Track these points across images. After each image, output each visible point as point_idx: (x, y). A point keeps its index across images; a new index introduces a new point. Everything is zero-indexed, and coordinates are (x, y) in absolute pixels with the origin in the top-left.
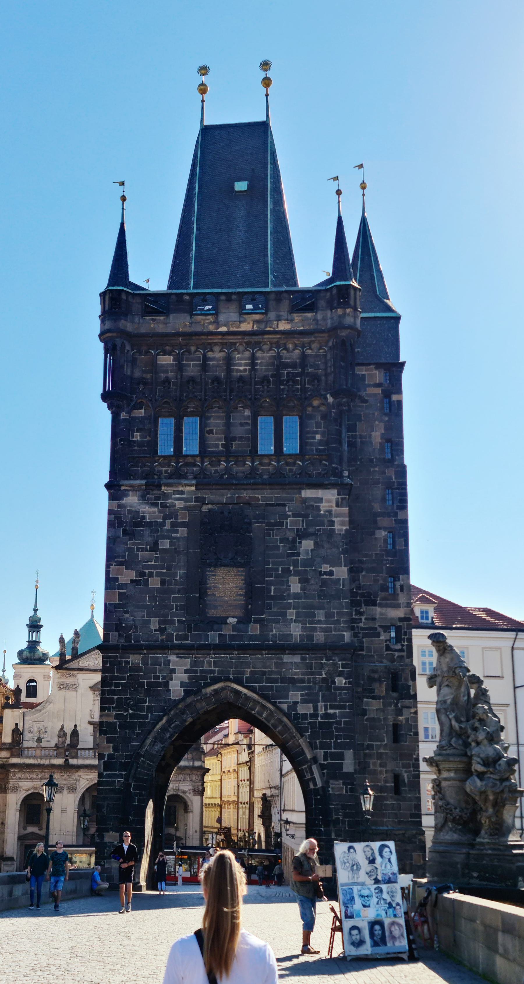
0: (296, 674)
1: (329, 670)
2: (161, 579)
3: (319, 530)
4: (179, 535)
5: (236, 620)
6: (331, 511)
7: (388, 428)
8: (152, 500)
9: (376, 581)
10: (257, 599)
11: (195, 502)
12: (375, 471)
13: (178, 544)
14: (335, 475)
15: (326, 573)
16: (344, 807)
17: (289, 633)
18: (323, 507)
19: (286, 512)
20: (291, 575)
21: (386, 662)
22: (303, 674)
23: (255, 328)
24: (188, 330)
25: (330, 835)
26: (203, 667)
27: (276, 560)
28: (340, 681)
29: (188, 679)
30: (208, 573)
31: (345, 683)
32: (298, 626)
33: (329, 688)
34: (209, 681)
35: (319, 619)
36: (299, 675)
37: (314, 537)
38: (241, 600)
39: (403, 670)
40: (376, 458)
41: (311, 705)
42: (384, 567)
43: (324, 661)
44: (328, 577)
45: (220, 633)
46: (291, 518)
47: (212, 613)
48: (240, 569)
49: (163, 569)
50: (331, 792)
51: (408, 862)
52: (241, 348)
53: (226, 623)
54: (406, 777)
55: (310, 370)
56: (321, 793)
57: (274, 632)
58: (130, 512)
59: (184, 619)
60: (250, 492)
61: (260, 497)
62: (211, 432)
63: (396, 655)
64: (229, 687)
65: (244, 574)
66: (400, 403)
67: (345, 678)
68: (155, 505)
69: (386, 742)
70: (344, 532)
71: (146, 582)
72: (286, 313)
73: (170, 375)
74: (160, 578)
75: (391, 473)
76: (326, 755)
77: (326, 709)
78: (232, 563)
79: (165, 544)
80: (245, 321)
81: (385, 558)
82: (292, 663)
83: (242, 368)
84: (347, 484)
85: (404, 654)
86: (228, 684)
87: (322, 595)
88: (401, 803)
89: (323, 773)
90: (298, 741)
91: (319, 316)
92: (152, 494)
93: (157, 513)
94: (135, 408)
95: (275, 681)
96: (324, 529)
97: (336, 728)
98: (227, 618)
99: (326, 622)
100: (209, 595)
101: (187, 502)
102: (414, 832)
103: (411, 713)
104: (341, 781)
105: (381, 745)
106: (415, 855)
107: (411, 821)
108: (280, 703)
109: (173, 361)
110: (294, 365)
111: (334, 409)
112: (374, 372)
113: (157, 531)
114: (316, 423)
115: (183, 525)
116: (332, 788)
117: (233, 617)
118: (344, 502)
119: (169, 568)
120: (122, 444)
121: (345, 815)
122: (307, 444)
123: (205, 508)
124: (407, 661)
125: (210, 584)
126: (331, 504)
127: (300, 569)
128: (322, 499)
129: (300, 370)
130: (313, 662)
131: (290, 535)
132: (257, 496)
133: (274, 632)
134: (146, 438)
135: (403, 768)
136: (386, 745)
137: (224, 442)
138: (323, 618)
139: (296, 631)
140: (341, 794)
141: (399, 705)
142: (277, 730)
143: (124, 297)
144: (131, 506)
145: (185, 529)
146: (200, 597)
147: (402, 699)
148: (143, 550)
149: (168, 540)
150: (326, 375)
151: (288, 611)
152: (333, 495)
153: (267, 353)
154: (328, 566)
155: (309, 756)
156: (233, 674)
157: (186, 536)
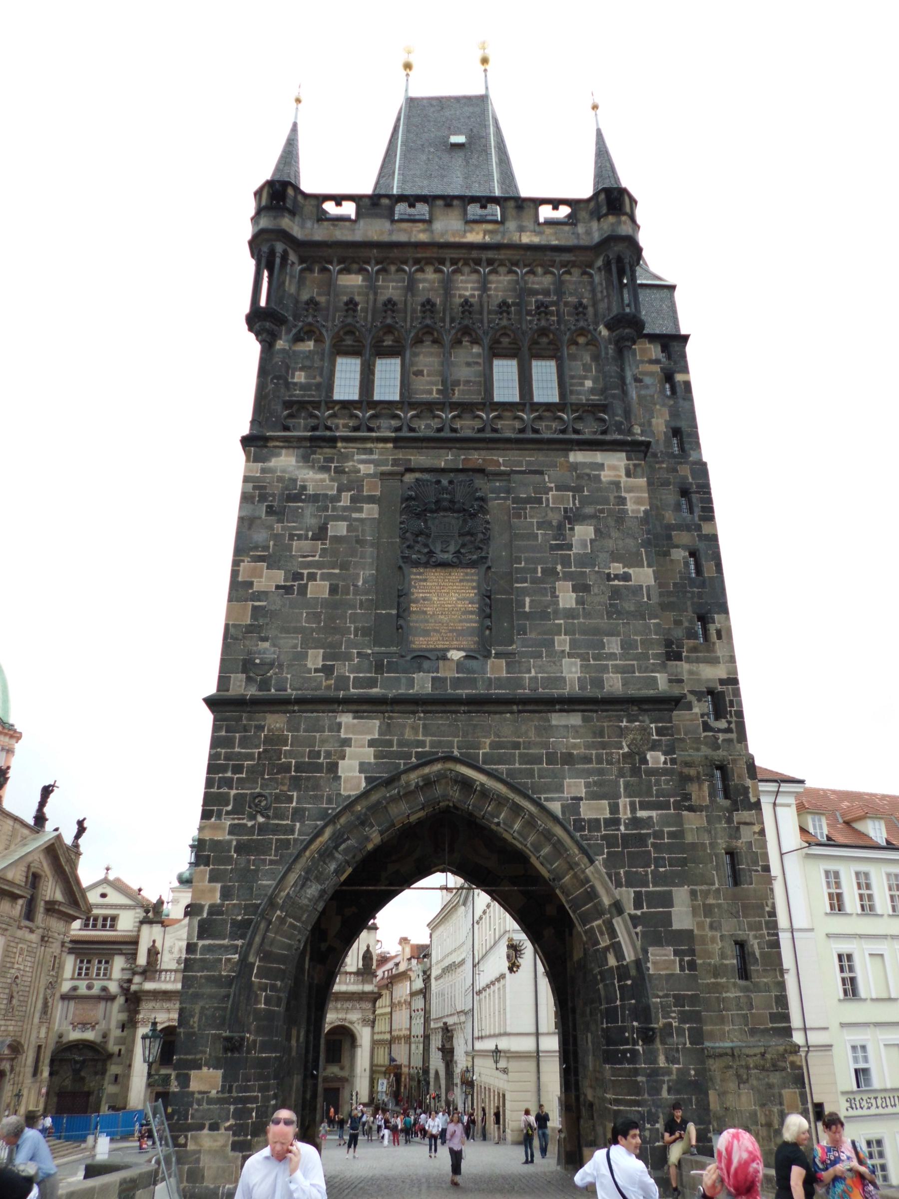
0: (575, 746)
1: (634, 739)
2: (331, 585)
3: (602, 511)
4: (363, 516)
5: (463, 654)
6: (619, 482)
7: (675, 414)
8: (319, 462)
9: (678, 623)
10: (497, 619)
11: (392, 465)
12: (661, 468)
13: (362, 530)
14: (620, 432)
15: (617, 577)
16: (679, 1000)
17: (559, 675)
18: (605, 476)
19: (545, 483)
20: (559, 579)
21: (705, 751)
22: (588, 746)
23: (487, 239)
24: (385, 238)
25: (655, 1061)
26: (403, 734)
27: (531, 555)
28: (656, 759)
29: (376, 757)
30: (413, 577)
31: (665, 763)
32: (576, 662)
33: (635, 772)
34: (414, 760)
35: (611, 651)
36: (580, 748)
37: (594, 521)
38: (471, 621)
39: (734, 761)
40: (661, 452)
41: (605, 802)
42: (689, 603)
43: (624, 724)
44: (621, 583)
45: (435, 675)
46: (554, 492)
47: (420, 643)
48: (469, 570)
49: (333, 568)
50: (651, 972)
51: (775, 1110)
52: (466, 270)
53: (445, 658)
54: (756, 946)
55: (570, 299)
56: (633, 972)
57: (533, 674)
58: (280, 479)
59: (369, 651)
60: (483, 452)
61: (501, 460)
62: (419, 373)
63: (721, 738)
64: (451, 770)
65: (475, 578)
66: (687, 385)
67: (665, 754)
68: (325, 469)
69: (717, 886)
70: (642, 515)
71: (303, 590)
72: (532, 223)
73: (357, 298)
74: (327, 583)
75: (684, 470)
76: (638, 895)
77: (633, 810)
78: (455, 560)
79: (339, 529)
80: (471, 231)
81: (688, 589)
82: (567, 726)
83: (467, 293)
84: (642, 443)
85: (734, 736)
86: (450, 765)
87: (613, 611)
88: (752, 995)
89: (637, 934)
90: (583, 872)
91: (581, 229)
92: (320, 454)
93: (328, 482)
94: (298, 339)
95: (537, 760)
96: (609, 510)
97: (653, 845)
98: (448, 650)
99: (623, 657)
100: (414, 612)
101: (378, 465)
102: (781, 1049)
103: (755, 833)
104: (671, 949)
105: (709, 890)
106: (786, 1092)
107: (773, 1029)
108: (547, 799)
109: (363, 280)
110: (546, 293)
111: (610, 343)
112: (648, 345)
113: (326, 509)
114: (584, 365)
115: (371, 499)
116: (654, 963)
117: (459, 649)
118: (639, 470)
119: (344, 566)
120: (275, 384)
121: (684, 1018)
122: (572, 392)
123: (409, 478)
124: (738, 746)
125: (418, 592)
126: (617, 473)
127: (573, 569)
128: (603, 465)
129: (555, 298)
130: (605, 724)
131: (555, 518)
132: (495, 458)
133: (533, 674)
134: (315, 378)
135: (750, 929)
136: (718, 890)
137: (440, 387)
138: (617, 650)
139: (571, 673)
140: (672, 975)
141: (735, 819)
142: (542, 853)
143: (290, 192)
144: (284, 471)
145: (375, 507)
146: (398, 616)
147: (737, 810)
148: (300, 537)
149: (346, 523)
150: (595, 304)
151: (556, 638)
152: (620, 459)
153: (505, 275)
154: (621, 565)
155: (606, 901)
156: (458, 748)
157: (376, 516)
